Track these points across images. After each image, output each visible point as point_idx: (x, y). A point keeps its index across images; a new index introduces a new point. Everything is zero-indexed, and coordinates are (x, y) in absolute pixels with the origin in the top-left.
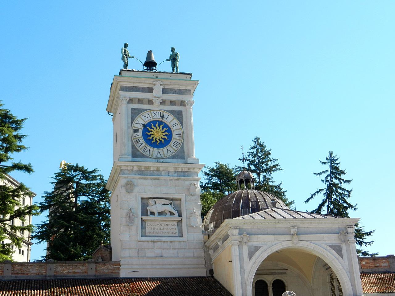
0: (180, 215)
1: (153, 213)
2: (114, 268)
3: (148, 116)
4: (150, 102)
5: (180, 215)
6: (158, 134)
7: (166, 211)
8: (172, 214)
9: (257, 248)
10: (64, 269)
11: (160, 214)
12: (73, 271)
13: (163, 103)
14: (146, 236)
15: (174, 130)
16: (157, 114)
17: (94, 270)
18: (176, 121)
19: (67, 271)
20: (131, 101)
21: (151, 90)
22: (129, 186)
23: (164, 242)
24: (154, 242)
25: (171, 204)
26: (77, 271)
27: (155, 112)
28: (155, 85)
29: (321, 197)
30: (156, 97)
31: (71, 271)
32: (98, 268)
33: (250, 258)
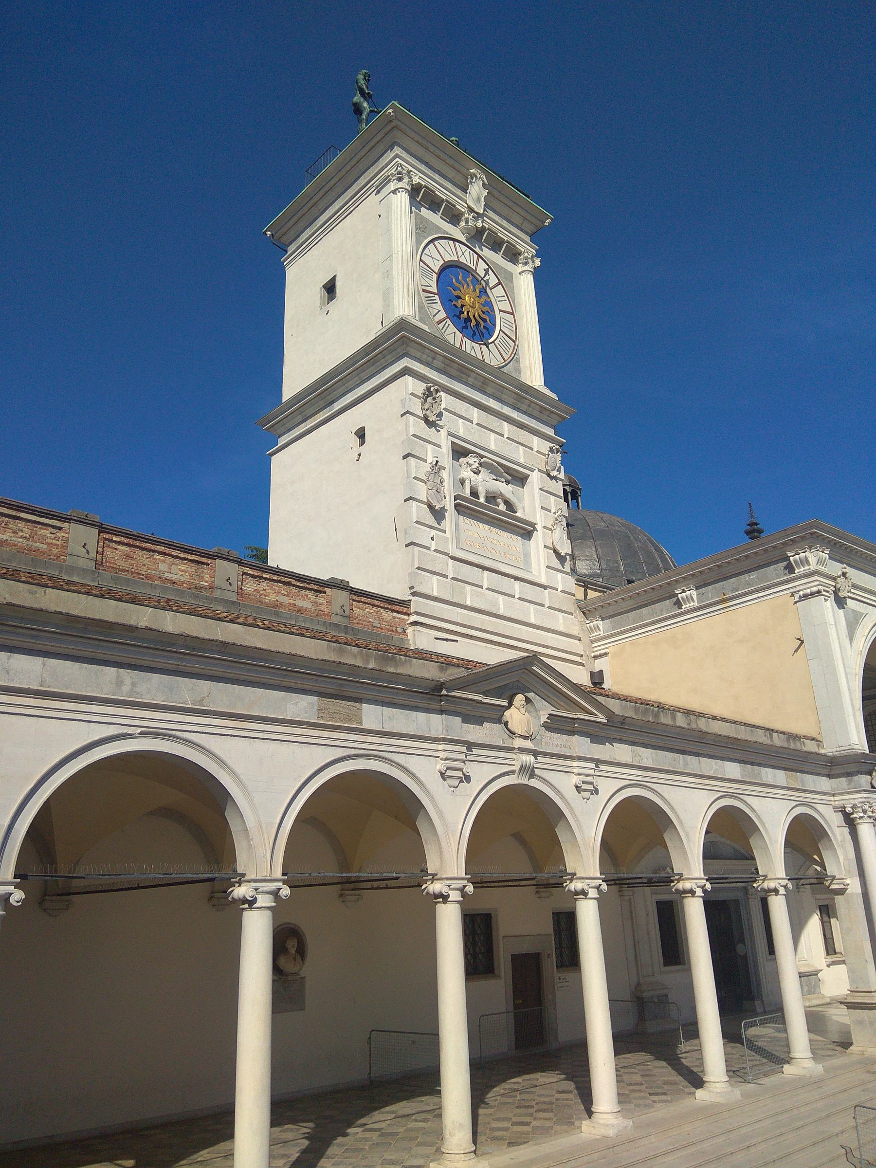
2: (394, 618)
3: (448, 248)
7: (499, 500)
10: (264, 590)
12: (292, 602)
15: (500, 311)
16: (467, 254)
19: (273, 597)
22: (430, 399)
26: (300, 603)
27: (464, 248)
28: (473, 176)
30: (471, 210)
31: (286, 600)
32: (357, 611)
33: (851, 636)
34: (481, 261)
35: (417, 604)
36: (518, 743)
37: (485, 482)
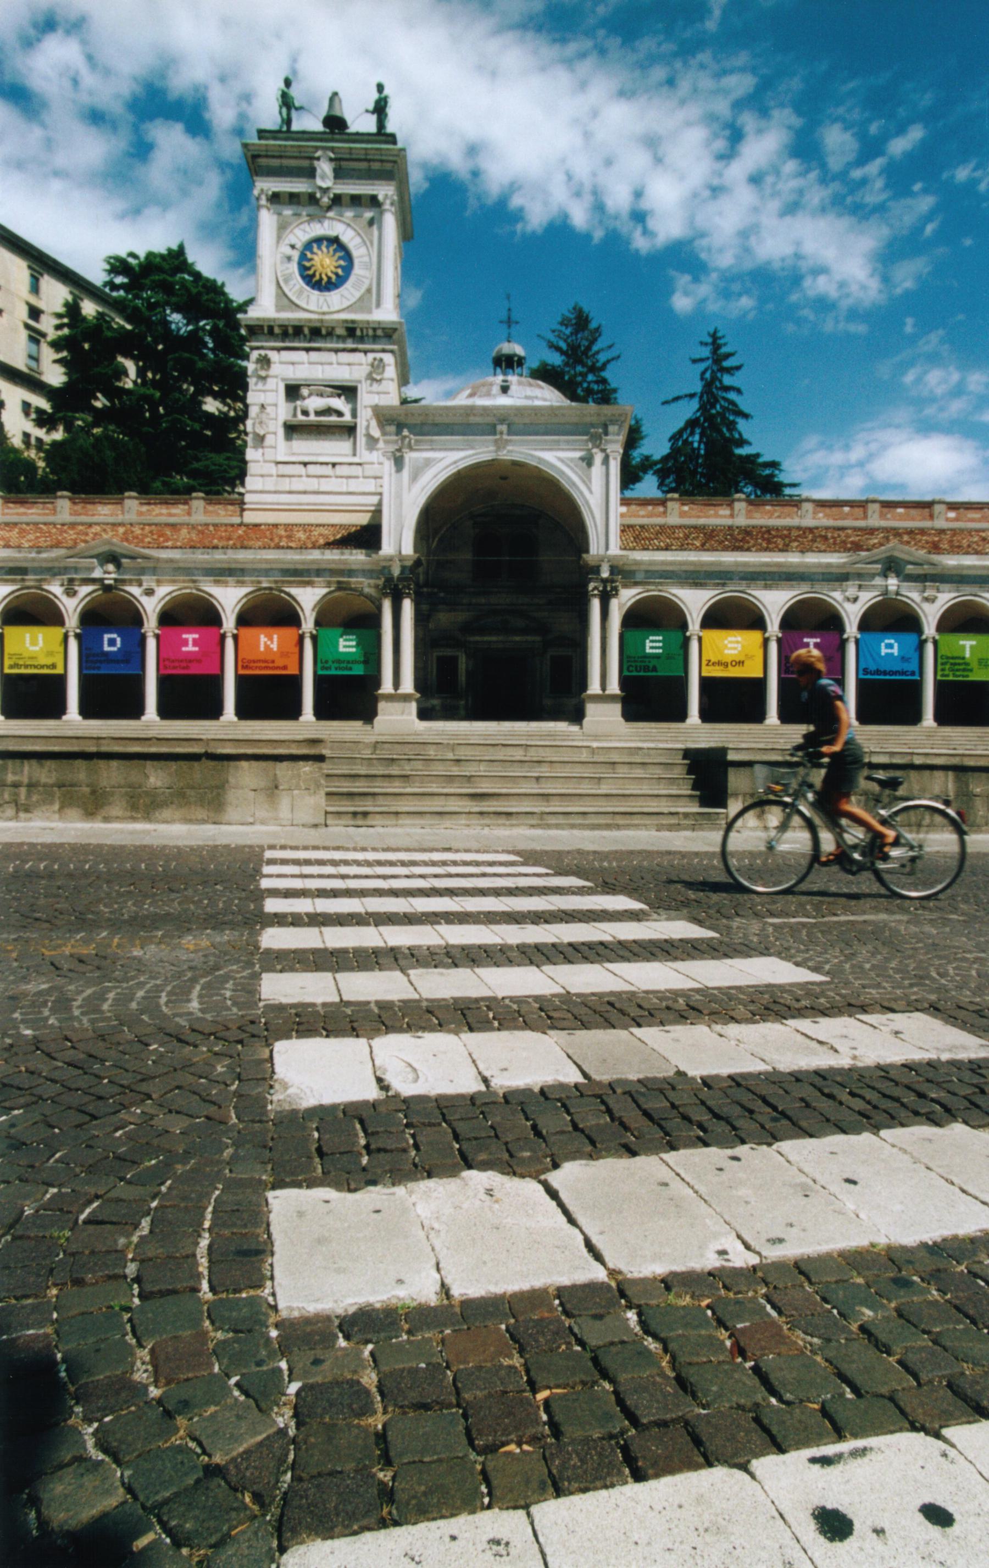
0: (354, 415)
1: (305, 413)
4: (312, 199)
5: (354, 415)
6: (325, 262)
8: (340, 414)
9: (428, 463)
11: (318, 413)
13: (337, 200)
14: (293, 454)
17: (202, 510)
18: (358, 240)
20: (275, 198)
21: (310, 173)
23: (322, 464)
24: (305, 464)
25: (339, 396)
29: (690, 409)
30: (320, 188)
34: (338, 226)
35: (248, 498)
36: (107, 576)
37: (314, 403)
